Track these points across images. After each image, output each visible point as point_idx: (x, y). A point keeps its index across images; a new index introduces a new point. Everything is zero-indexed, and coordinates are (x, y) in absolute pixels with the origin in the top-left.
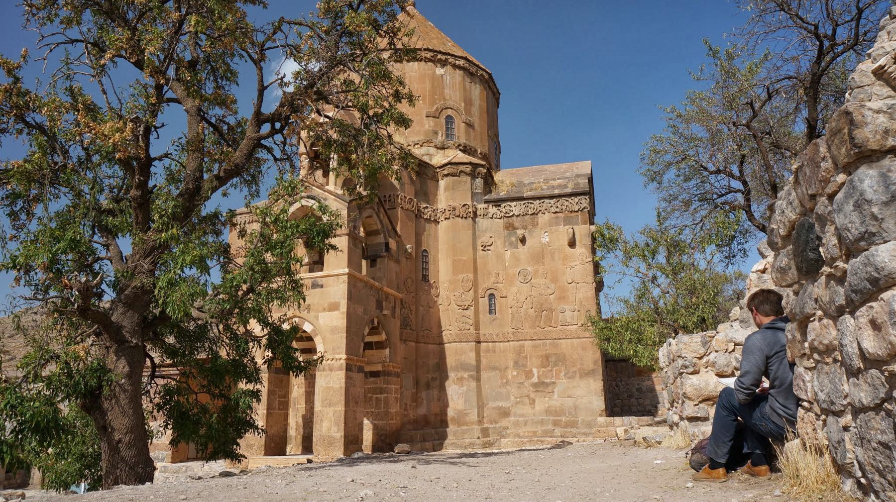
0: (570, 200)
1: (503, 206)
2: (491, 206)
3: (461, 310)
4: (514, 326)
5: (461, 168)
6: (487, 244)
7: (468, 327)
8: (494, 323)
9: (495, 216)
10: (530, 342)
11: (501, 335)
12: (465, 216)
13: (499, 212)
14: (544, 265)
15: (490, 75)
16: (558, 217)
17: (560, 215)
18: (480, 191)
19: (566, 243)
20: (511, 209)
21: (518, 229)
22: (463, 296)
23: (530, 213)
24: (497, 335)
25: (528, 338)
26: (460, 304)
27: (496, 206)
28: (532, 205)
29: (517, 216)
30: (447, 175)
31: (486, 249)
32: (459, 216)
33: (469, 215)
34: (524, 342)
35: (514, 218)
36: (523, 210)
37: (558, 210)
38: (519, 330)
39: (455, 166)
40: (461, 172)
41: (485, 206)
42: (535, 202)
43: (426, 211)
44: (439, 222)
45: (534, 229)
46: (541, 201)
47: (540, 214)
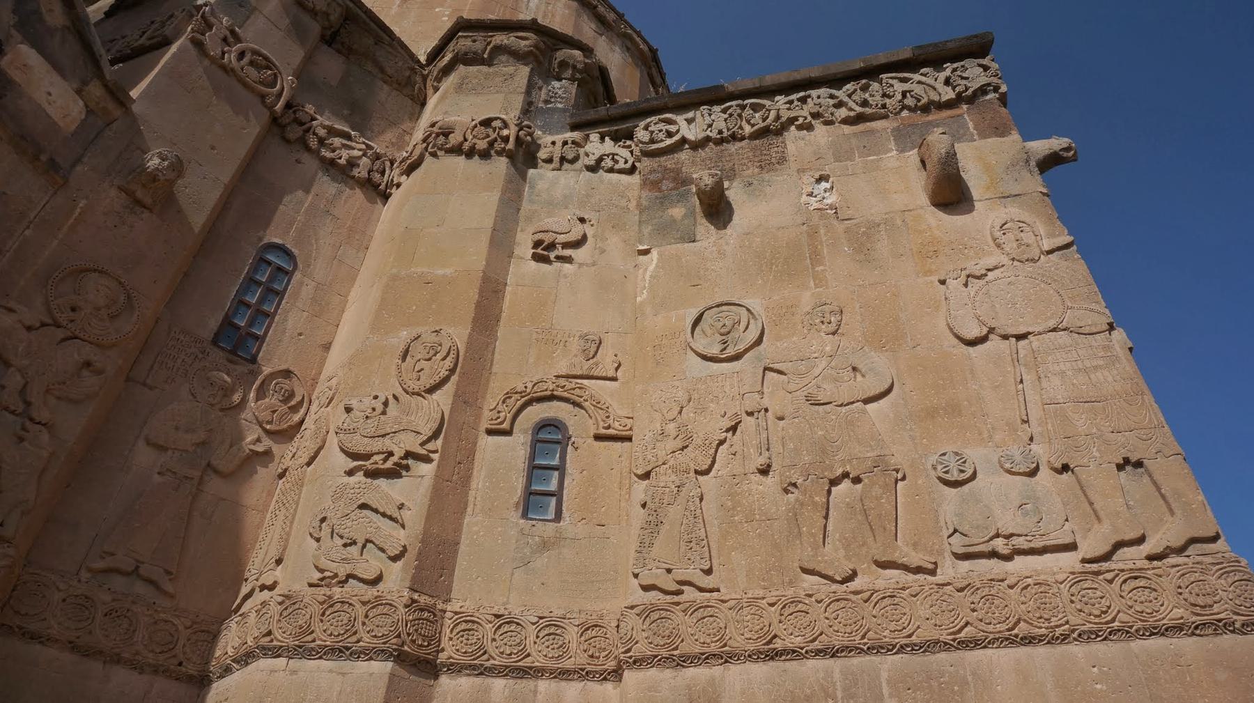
0: (917, 77)
2: (594, 137)
3: (359, 476)
4: (654, 575)
5: (500, 39)
6: (562, 239)
7: (371, 564)
8: (540, 562)
9: (608, 163)
10: (759, 670)
11: (572, 634)
12: (482, 145)
14: (820, 281)
15: (654, 52)
19: (924, 200)
24: (551, 626)
25: (738, 642)
26: (361, 445)
27: (616, 138)
29: (697, 145)
30: (447, 71)
34: (716, 671)
35: (684, 155)
38: (690, 594)
39: (479, 36)
40: (499, 50)
41: (576, 135)
43: (337, 141)
44: (386, 197)
45: (766, 176)
46: (794, 97)
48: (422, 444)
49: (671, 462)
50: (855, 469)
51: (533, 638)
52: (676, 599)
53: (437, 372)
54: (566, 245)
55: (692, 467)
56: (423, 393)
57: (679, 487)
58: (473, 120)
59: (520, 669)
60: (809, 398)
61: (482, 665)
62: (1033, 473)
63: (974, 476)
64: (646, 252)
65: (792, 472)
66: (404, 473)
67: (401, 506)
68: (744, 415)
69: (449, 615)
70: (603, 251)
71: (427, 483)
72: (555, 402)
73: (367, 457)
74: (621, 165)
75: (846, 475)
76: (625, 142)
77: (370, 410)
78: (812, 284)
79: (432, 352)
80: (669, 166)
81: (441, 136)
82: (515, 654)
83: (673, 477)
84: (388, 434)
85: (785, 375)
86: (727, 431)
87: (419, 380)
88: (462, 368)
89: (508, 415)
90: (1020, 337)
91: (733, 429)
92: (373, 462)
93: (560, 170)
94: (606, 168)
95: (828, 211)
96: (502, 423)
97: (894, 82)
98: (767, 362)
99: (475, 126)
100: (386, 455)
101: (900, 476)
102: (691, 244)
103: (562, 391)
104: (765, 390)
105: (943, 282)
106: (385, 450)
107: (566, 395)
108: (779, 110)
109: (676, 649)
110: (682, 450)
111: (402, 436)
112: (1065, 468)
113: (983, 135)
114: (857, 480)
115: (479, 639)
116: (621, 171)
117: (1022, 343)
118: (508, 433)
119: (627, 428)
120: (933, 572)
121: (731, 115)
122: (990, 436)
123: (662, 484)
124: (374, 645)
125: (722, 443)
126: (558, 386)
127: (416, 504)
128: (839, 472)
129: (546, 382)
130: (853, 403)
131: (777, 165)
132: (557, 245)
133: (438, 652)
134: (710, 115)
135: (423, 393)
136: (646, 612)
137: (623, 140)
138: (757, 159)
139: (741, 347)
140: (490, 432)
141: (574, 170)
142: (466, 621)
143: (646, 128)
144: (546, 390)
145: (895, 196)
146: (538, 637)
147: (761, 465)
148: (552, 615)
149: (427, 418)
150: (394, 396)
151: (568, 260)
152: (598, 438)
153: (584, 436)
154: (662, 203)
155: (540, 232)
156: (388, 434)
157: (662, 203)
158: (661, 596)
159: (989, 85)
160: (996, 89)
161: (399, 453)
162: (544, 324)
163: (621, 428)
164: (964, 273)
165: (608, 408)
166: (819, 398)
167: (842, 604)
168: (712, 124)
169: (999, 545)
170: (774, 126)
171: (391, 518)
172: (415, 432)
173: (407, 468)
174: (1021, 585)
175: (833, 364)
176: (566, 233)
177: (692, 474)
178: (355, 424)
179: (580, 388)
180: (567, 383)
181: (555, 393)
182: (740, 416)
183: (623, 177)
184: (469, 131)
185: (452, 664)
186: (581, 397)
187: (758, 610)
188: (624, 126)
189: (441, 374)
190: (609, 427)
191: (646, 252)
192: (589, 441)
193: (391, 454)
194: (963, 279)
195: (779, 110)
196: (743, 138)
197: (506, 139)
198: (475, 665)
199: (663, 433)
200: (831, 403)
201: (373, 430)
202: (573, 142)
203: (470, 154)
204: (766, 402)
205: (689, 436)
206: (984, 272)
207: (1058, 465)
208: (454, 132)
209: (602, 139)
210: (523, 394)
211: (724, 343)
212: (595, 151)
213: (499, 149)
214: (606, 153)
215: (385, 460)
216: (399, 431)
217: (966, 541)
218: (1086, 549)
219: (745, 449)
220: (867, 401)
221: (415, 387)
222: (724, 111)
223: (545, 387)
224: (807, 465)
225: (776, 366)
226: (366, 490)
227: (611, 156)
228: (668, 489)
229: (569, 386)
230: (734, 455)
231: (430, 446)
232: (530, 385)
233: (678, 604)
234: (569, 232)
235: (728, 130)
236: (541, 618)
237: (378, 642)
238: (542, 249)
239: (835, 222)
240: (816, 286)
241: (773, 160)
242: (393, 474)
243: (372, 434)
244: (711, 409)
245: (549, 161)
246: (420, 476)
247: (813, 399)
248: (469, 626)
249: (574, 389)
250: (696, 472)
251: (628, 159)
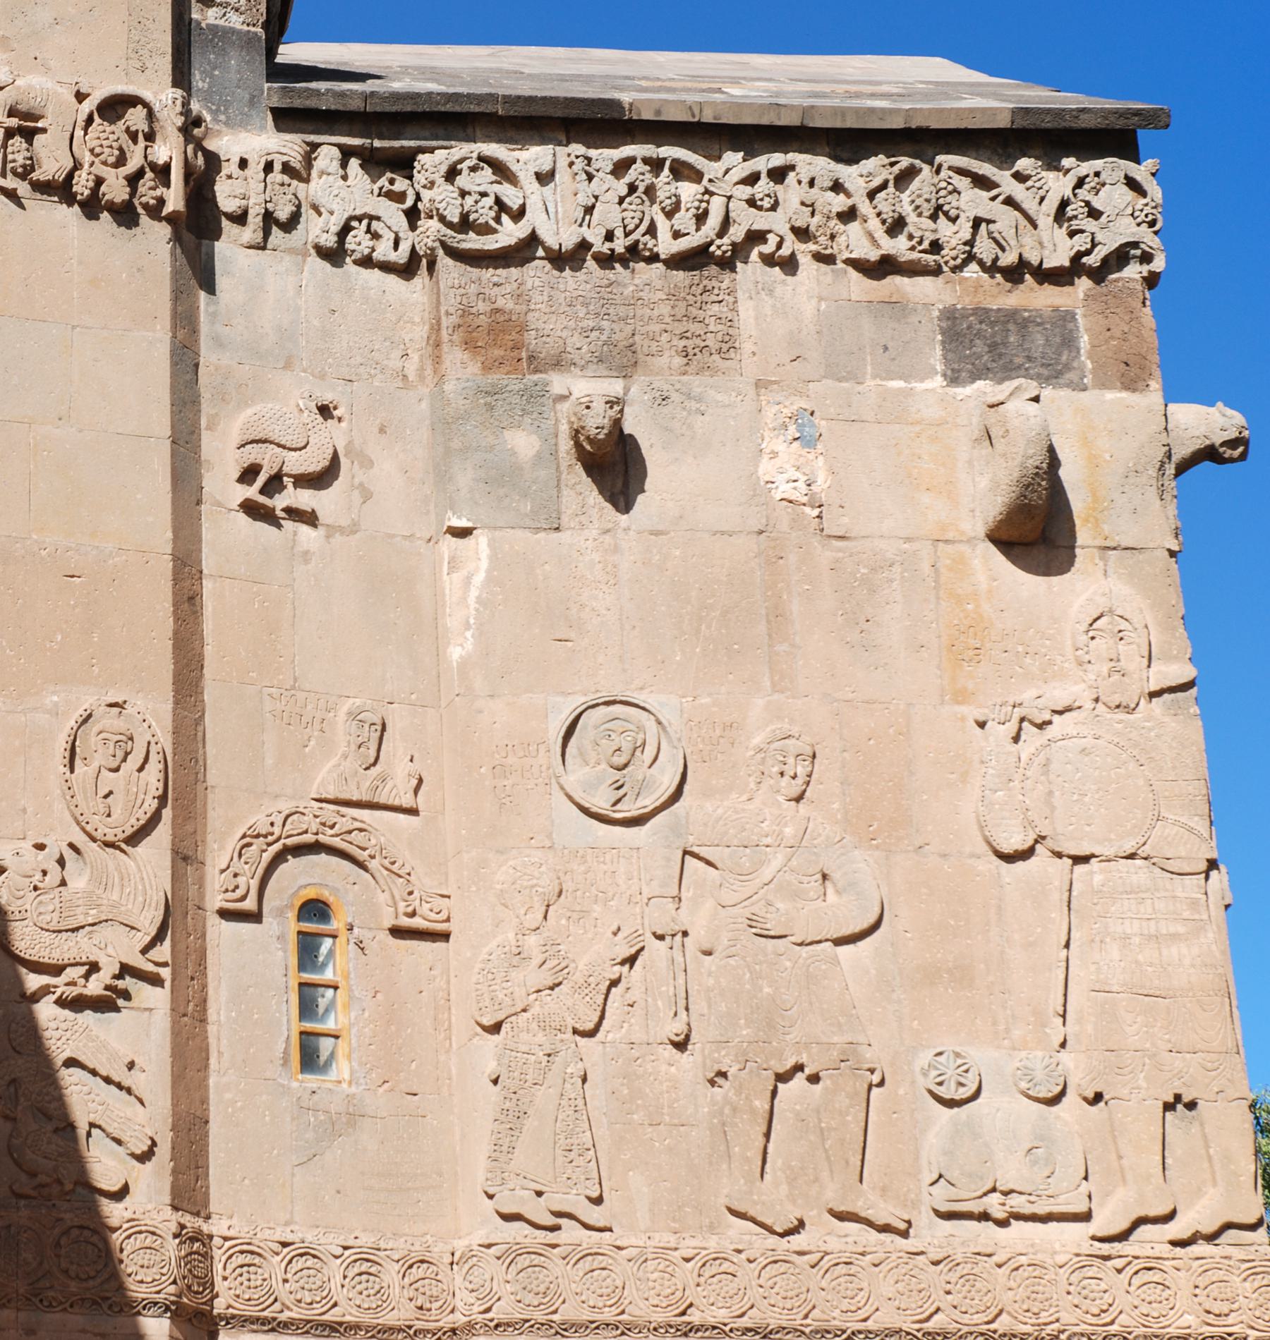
0: (1004, 178)
1: (432, 163)
2: (327, 157)
6: (297, 463)
9: (358, 241)
12: (115, 190)
13: (393, 215)
16: (897, 307)
17: (922, 287)
18: (235, 21)
20: (512, 197)
21: (558, 363)
22: (79, 881)
23: (666, 245)
27: (374, 162)
28: (688, 191)
31: (279, 502)
32: (61, 190)
33: (148, 191)
35: (537, 272)
36: (608, 215)
37: (899, 247)
38: (570, 1233)
41: (289, 146)
42: (711, 169)
45: (696, 383)
47: (751, 271)
48: (144, 951)
49: (535, 1010)
50: (813, 1062)
51: (339, 1278)
52: (551, 1237)
53: (139, 802)
54: (304, 481)
55: (571, 1023)
56: (123, 846)
57: (549, 1055)
58: (80, 97)
59: (324, 1325)
60: (754, 924)
61: (274, 1319)
62: (1054, 1100)
63: (976, 1095)
64: (463, 533)
65: (723, 1053)
66: (121, 1002)
67: (131, 1066)
68: (649, 936)
69: (217, 1241)
70: (367, 495)
71: (161, 1021)
72: (323, 855)
73: (57, 970)
74: (384, 251)
75: (799, 1068)
76: (392, 182)
77: (39, 876)
78: (767, 683)
79: (120, 754)
80: (500, 303)
81: (18, 139)
82: (318, 1303)
83: (540, 1038)
84: (83, 927)
85: (717, 868)
86: (623, 963)
87: (109, 815)
88: (174, 789)
89: (251, 881)
90: (1079, 860)
91: (631, 960)
92: (68, 980)
93: (264, 248)
94: (357, 256)
95: (807, 510)
96: (243, 898)
97: (962, 183)
98: (691, 842)
99: (89, 121)
100: (87, 967)
101: (876, 1078)
102: (556, 535)
103: (332, 836)
104: (684, 895)
105: (982, 725)
106: (84, 959)
107: (337, 842)
108: (729, 198)
109: (555, 1312)
110: (552, 988)
111: (105, 932)
112: (1098, 1097)
113: (1103, 385)
114: (814, 1079)
115: (264, 1280)
116: (386, 267)
117: (1080, 869)
118: (254, 917)
119: (443, 916)
120: (905, 1234)
121: (632, 188)
122: (1007, 1030)
123: (524, 1048)
124: (144, 1296)
125: (614, 983)
126: (324, 824)
127: (150, 1059)
128: (789, 1064)
129: (304, 814)
130: (819, 942)
131: (716, 357)
132: (285, 479)
133: (212, 1299)
134: (590, 177)
135: (123, 846)
136: (510, 1256)
137: (389, 175)
138: (679, 327)
139: (648, 802)
140: (225, 914)
141: (291, 251)
142: (242, 1252)
143: (452, 174)
144: (306, 832)
145: (926, 499)
146: (345, 1277)
147: (677, 1035)
148: (358, 1243)
149: (141, 899)
150: (71, 846)
151: (310, 518)
152: (397, 932)
153: (372, 925)
154: (490, 407)
155: (251, 442)
156: (83, 927)
157: (490, 407)
158: (528, 1229)
159: (1135, 245)
160: (1146, 258)
161: (108, 969)
162: (281, 677)
163: (433, 916)
164: (1018, 713)
165: (409, 874)
166: (768, 926)
167: (782, 1267)
168: (593, 207)
169: (994, 1204)
170: (719, 247)
171: (119, 1086)
172: (127, 925)
173: (126, 995)
174: (1012, 1264)
175: (794, 863)
176: (300, 449)
177: (569, 1035)
178: (19, 902)
179: (361, 830)
180: (339, 819)
181: (321, 838)
182: (641, 938)
183: (392, 280)
184: (79, 133)
185: (233, 1317)
186: (364, 849)
187: (668, 1266)
188: (397, 144)
189: (146, 805)
190: (413, 914)
191: (463, 533)
192: (382, 935)
193: (94, 968)
194: (1012, 727)
195: (729, 198)
196: (654, 258)
197: (163, 173)
198: (266, 1318)
199: (519, 954)
200: (785, 936)
201: (56, 916)
202: (287, 169)
203: (92, 207)
204: (685, 919)
205: (563, 965)
206: (1047, 717)
207: (1091, 1095)
208: (44, 130)
209: (344, 165)
210: (270, 839)
211: (618, 788)
212: (334, 207)
213: (152, 202)
214: (358, 212)
215: (87, 976)
216: (100, 922)
217: (954, 1193)
218: (1099, 1225)
219: (650, 1000)
220: (840, 942)
221: (107, 830)
222: (621, 168)
223: (304, 827)
224: (745, 1044)
225: (702, 851)
226: (69, 1033)
227: (365, 222)
228: (533, 1057)
229: (343, 824)
230: (632, 1006)
231: (155, 954)
232: (279, 820)
233: (554, 1246)
234: (304, 447)
235: (627, 235)
236: (346, 1248)
237: (148, 1290)
238: (262, 492)
239: (816, 542)
240: (776, 688)
241: (711, 341)
242: (103, 1004)
243: (53, 926)
244: (595, 915)
245: (240, 218)
246: (146, 1009)
247: (759, 925)
248: (248, 1259)
249: (350, 832)
250: (575, 1031)
251: (401, 235)
